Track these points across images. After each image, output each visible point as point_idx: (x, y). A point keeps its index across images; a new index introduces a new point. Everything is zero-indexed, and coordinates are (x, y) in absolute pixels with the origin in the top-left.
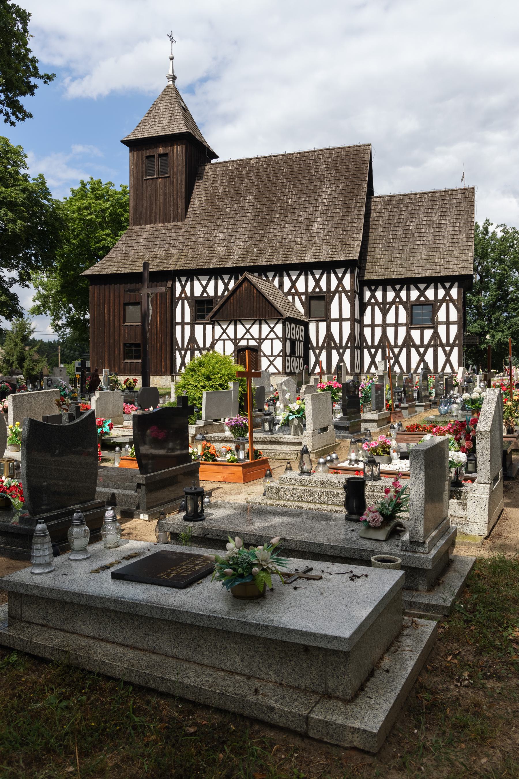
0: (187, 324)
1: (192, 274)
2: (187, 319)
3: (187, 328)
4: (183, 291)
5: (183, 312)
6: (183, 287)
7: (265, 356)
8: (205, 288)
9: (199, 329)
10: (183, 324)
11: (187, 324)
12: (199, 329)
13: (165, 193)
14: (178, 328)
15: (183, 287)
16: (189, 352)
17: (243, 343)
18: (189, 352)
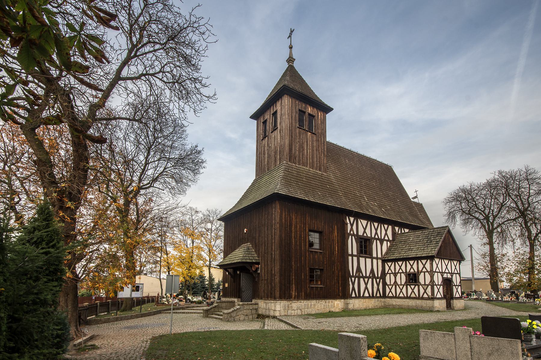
0: (355, 256)
1: (358, 216)
2: (355, 253)
3: (355, 259)
4: (352, 229)
5: (352, 246)
6: (352, 225)
7: (455, 285)
8: (365, 229)
9: (362, 260)
10: (352, 255)
11: (355, 256)
12: (362, 260)
13: (313, 147)
14: (350, 258)
15: (352, 225)
16: (357, 279)
17: (445, 276)
18: (357, 279)
